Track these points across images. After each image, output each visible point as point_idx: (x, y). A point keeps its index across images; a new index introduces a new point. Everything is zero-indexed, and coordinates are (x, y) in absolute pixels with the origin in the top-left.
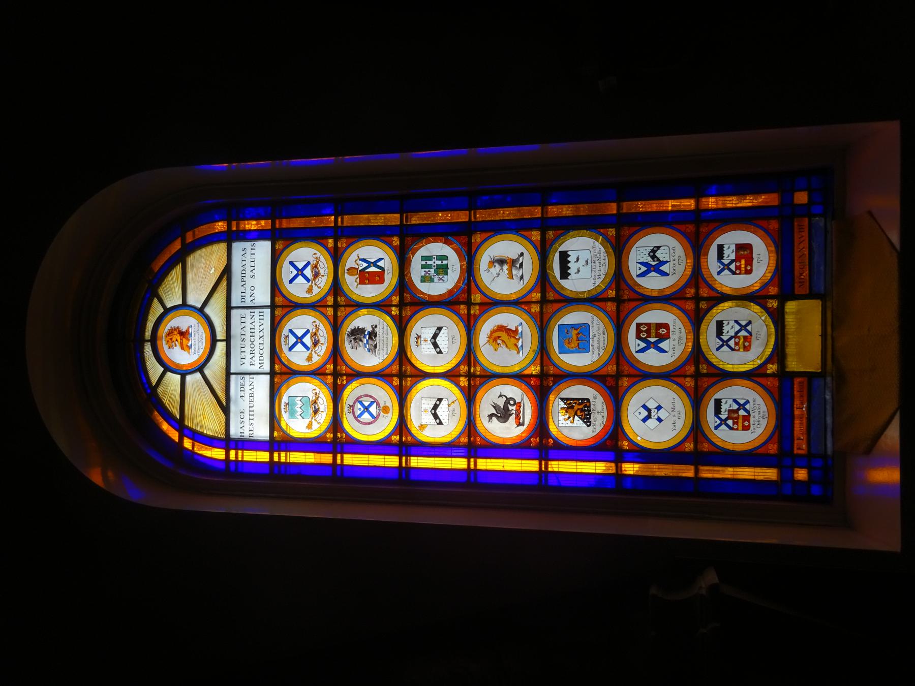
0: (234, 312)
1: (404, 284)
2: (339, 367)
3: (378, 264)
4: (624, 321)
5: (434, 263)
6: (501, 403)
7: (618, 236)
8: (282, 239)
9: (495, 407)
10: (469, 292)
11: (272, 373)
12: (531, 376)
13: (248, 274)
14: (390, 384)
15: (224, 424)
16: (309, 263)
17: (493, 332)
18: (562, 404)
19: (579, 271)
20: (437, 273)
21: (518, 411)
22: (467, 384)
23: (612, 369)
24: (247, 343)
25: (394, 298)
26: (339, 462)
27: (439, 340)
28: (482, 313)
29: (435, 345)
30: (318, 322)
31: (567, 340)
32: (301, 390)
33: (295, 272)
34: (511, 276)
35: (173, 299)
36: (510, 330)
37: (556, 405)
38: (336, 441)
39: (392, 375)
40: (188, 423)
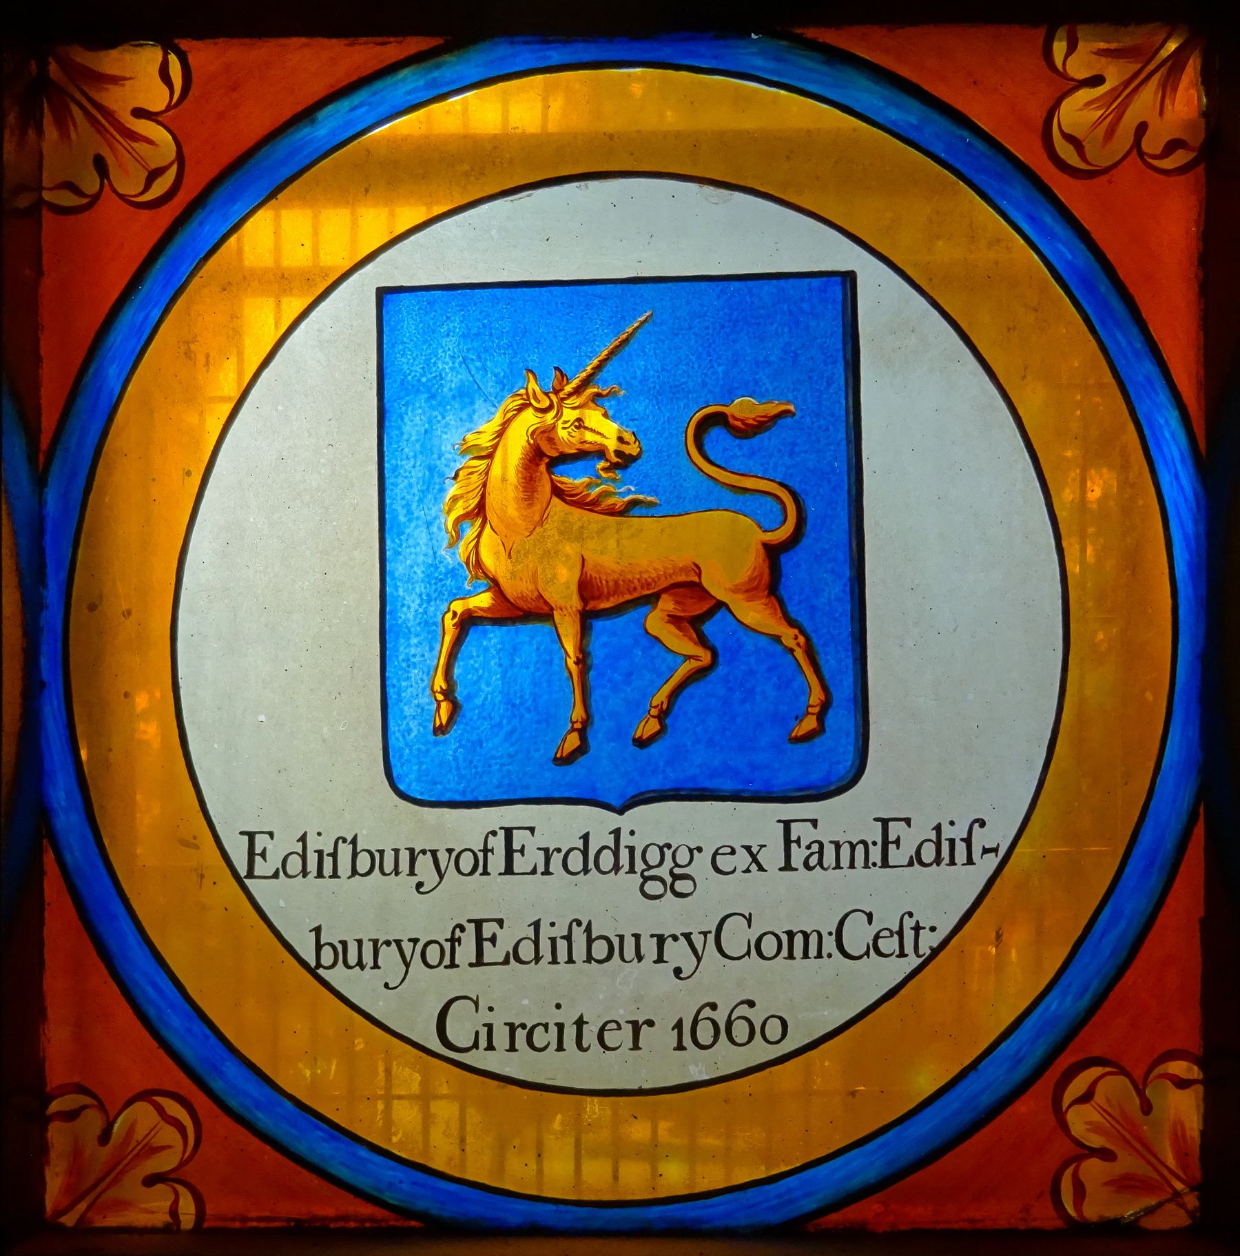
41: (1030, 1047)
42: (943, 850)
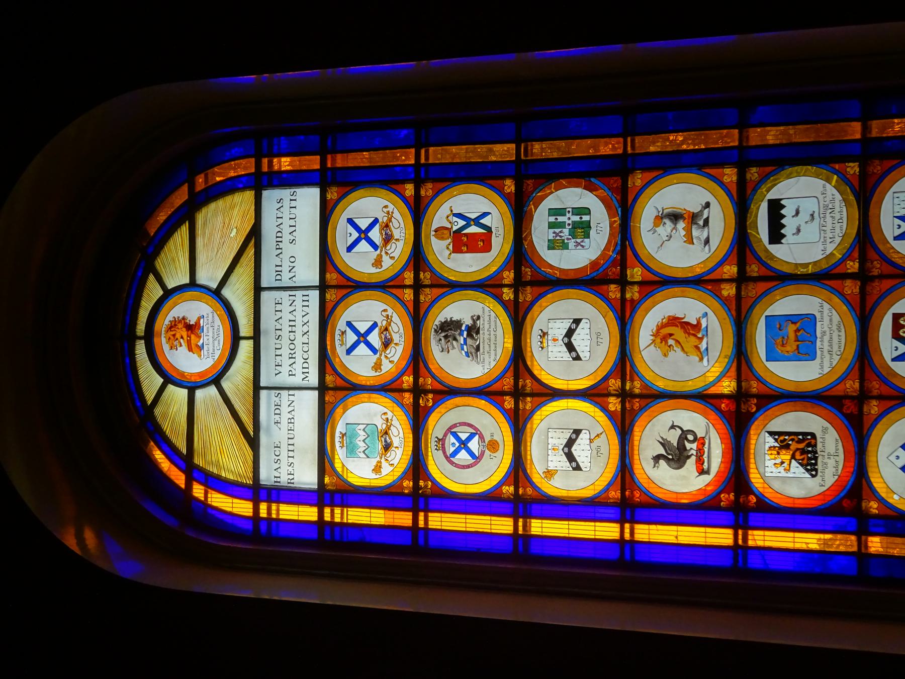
0: (264, 295)
1: (521, 252)
2: (421, 380)
3: (481, 221)
4: (872, 310)
5: (569, 219)
6: (673, 437)
7: (864, 175)
8: (336, 184)
9: (664, 444)
10: (624, 265)
11: (322, 388)
12: (721, 396)
13: (286, 238)
14: (500, 406)
15: (251, 463)
16: (376, 221)
17: (660, 327)
18: (771, 441)
19: (799, 230)
20: (573, 235)
21: (700, 451)
22: (619, 407)
23: (852, 386)
24: (285, 342)
25: (506, 274)
26: (421, 524)
27: (576, 340)
28: (644, 296)
29: (570, 347)
30: (390, 311)
31: (779, 341)
32: (365, 414)
33: (355, 235)
34: (690, 240)
35: (177, 276)
36: (688, 323)
37: (761, 442)
38: (417, 491)
39: (503, 393)
40: (198, 461)
41: (841, 297)
42: (822, 306)
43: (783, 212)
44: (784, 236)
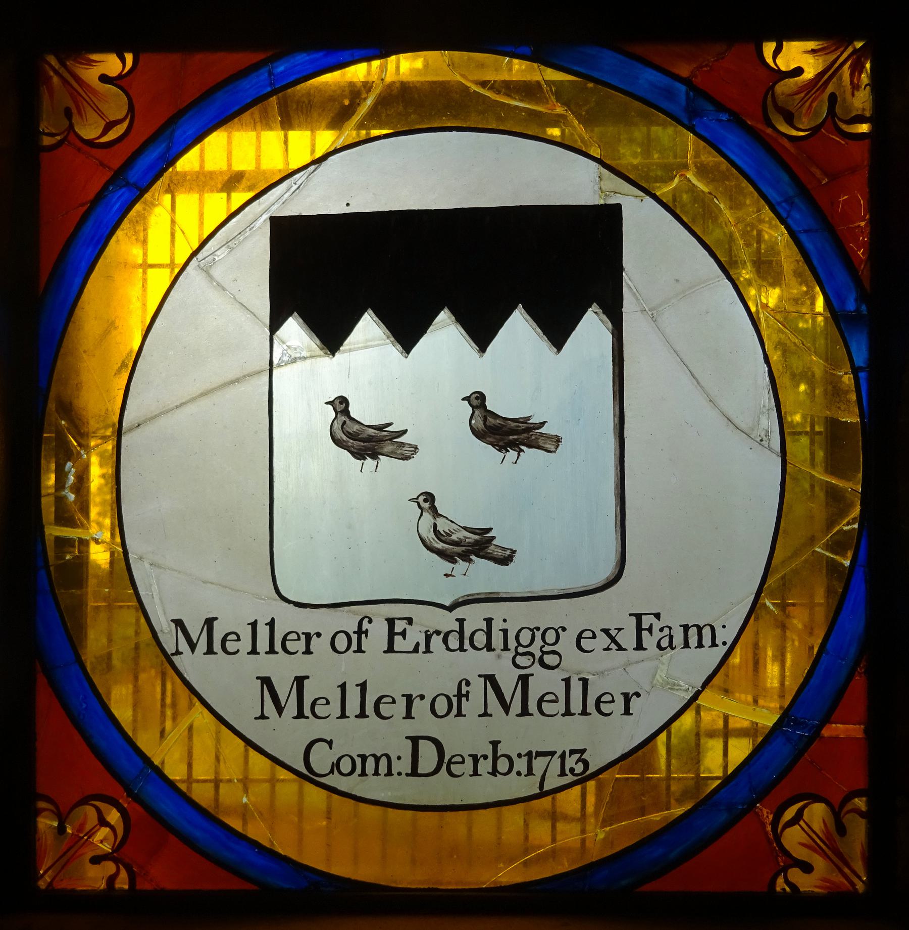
43: (519, 328)
44: (332, 337)
